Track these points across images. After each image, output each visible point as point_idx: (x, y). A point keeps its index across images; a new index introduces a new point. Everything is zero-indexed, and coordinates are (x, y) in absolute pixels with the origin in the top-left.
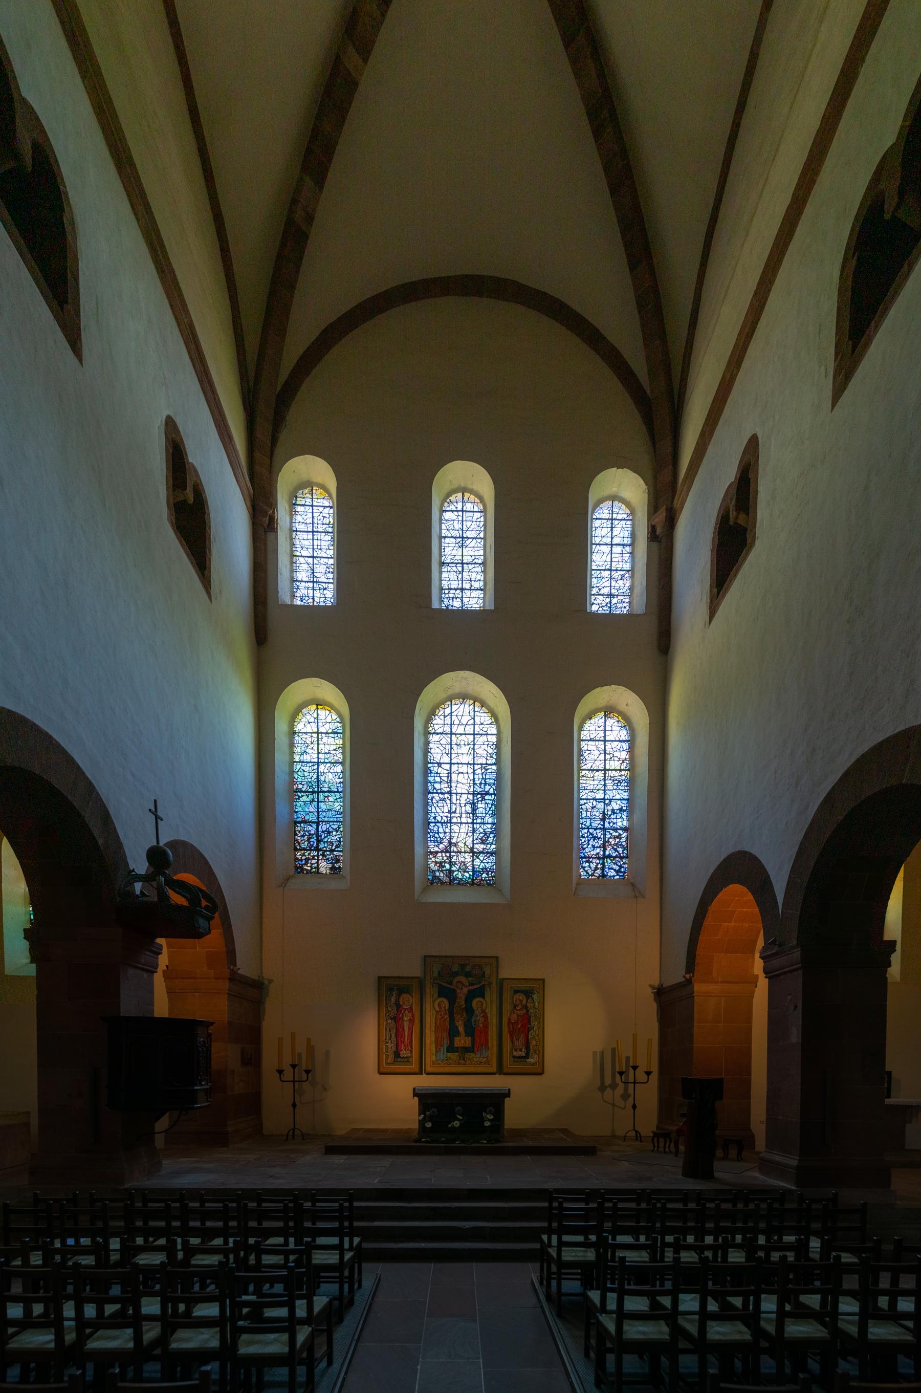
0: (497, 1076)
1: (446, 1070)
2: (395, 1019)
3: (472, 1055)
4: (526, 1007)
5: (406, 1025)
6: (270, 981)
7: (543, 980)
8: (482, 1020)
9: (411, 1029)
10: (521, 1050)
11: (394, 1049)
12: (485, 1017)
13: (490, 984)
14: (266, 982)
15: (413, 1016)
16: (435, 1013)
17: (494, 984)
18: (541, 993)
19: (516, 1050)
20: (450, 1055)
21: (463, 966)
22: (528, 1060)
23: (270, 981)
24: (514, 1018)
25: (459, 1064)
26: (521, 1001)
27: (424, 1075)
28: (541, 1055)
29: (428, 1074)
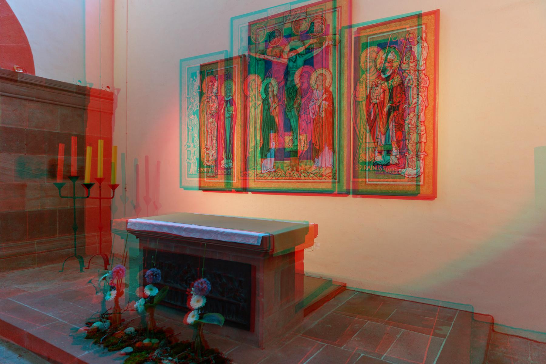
0: (350, 199)
1: (275, 186)
2: (217, 116)
3: (310, 163)
4: (399, 71)
5: (228, 122)
6: (119, 90)
7: (436, 13)
8: (325, 104)
9: (232, 128)
10: (389, 152)
11: (215, 157)
12: (330, 99)
13: (337, 44)
14: (116, 92)
15: (235, 110)
16: (260, 102)
17: (345, 41)
18: (431, 38)
19: (380, 152)
20: (279, 164)
21: (297, 23)
22: (403, 170)
23: (119, 90)
24: (377, 95)
25: (291, 177)
26: (391, 62)
27: (250, 193)
28: (429, 160)
29: (255, 192)
